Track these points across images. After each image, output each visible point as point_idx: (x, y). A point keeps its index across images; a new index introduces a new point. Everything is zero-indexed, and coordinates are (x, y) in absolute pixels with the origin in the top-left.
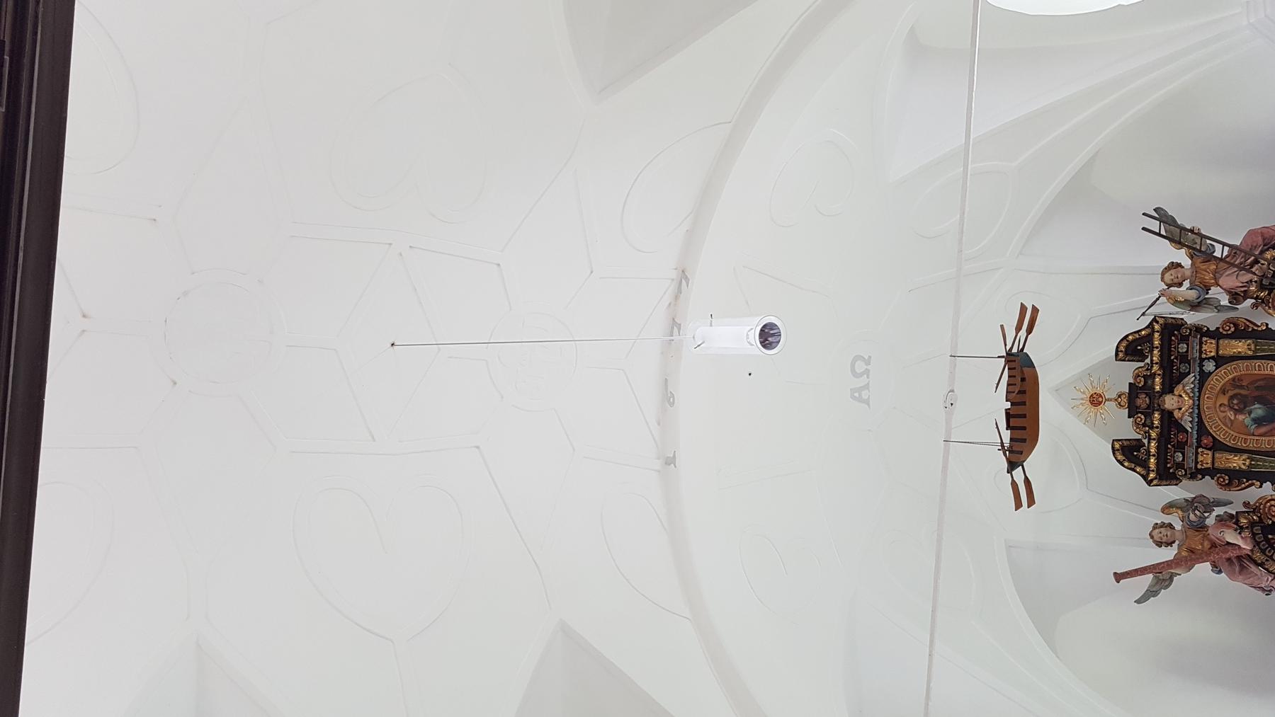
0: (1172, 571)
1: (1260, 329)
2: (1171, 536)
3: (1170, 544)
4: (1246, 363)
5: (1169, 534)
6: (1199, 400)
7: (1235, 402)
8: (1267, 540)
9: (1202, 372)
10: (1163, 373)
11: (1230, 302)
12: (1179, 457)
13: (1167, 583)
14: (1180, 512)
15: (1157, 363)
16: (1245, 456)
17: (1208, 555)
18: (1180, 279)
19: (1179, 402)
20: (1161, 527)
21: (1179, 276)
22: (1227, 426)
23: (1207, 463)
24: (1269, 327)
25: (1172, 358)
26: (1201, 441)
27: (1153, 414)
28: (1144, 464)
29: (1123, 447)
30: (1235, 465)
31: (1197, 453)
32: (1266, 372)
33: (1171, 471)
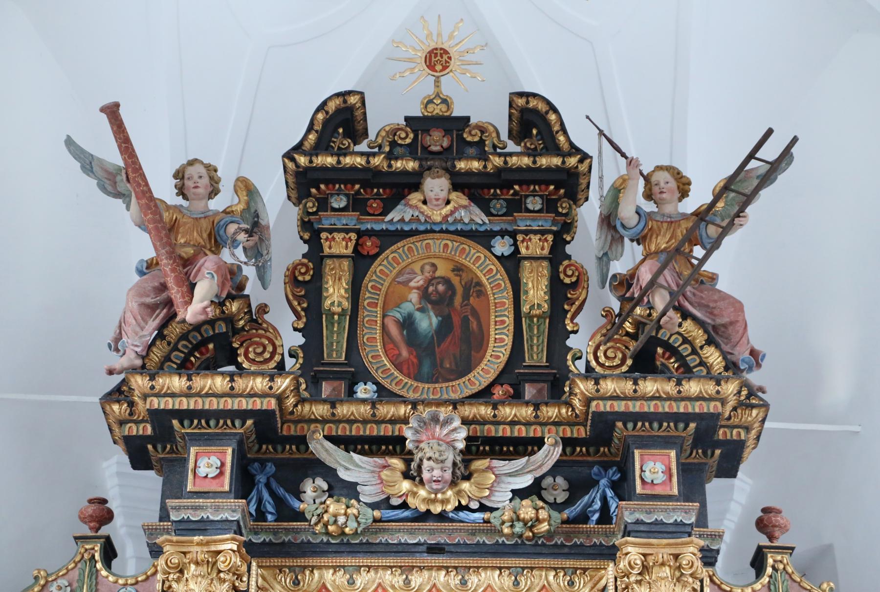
0: (134, 199)
1: (567, 321)
2: (194, 194)
3: (182, 191)
4: (509, 303)
5: (200, 191)
6: (441, 231)
7: (441, 288)
8: (204, 342)
9: (492, 234)
10: (488, 174)
11: (614, 276)
12: (339, 202)
13: (109, 188)
14: (241, 207)
15: (506, 162)
16: (346, 304)
17: (172, 254)
18: (659, 196)
19: (437, 200)
20: (211, 178)
21: (664, 196)
22: (400, 273)
23: (330, 248)
24: (572, 336)
25: (517, 187)
26: (370, 236)
27: (415, 159)
28: (322, 146)
29: (350, 109)
30: (331, 290)
31: (347, 231)
32: (492, 333)
33: (313, 191)
